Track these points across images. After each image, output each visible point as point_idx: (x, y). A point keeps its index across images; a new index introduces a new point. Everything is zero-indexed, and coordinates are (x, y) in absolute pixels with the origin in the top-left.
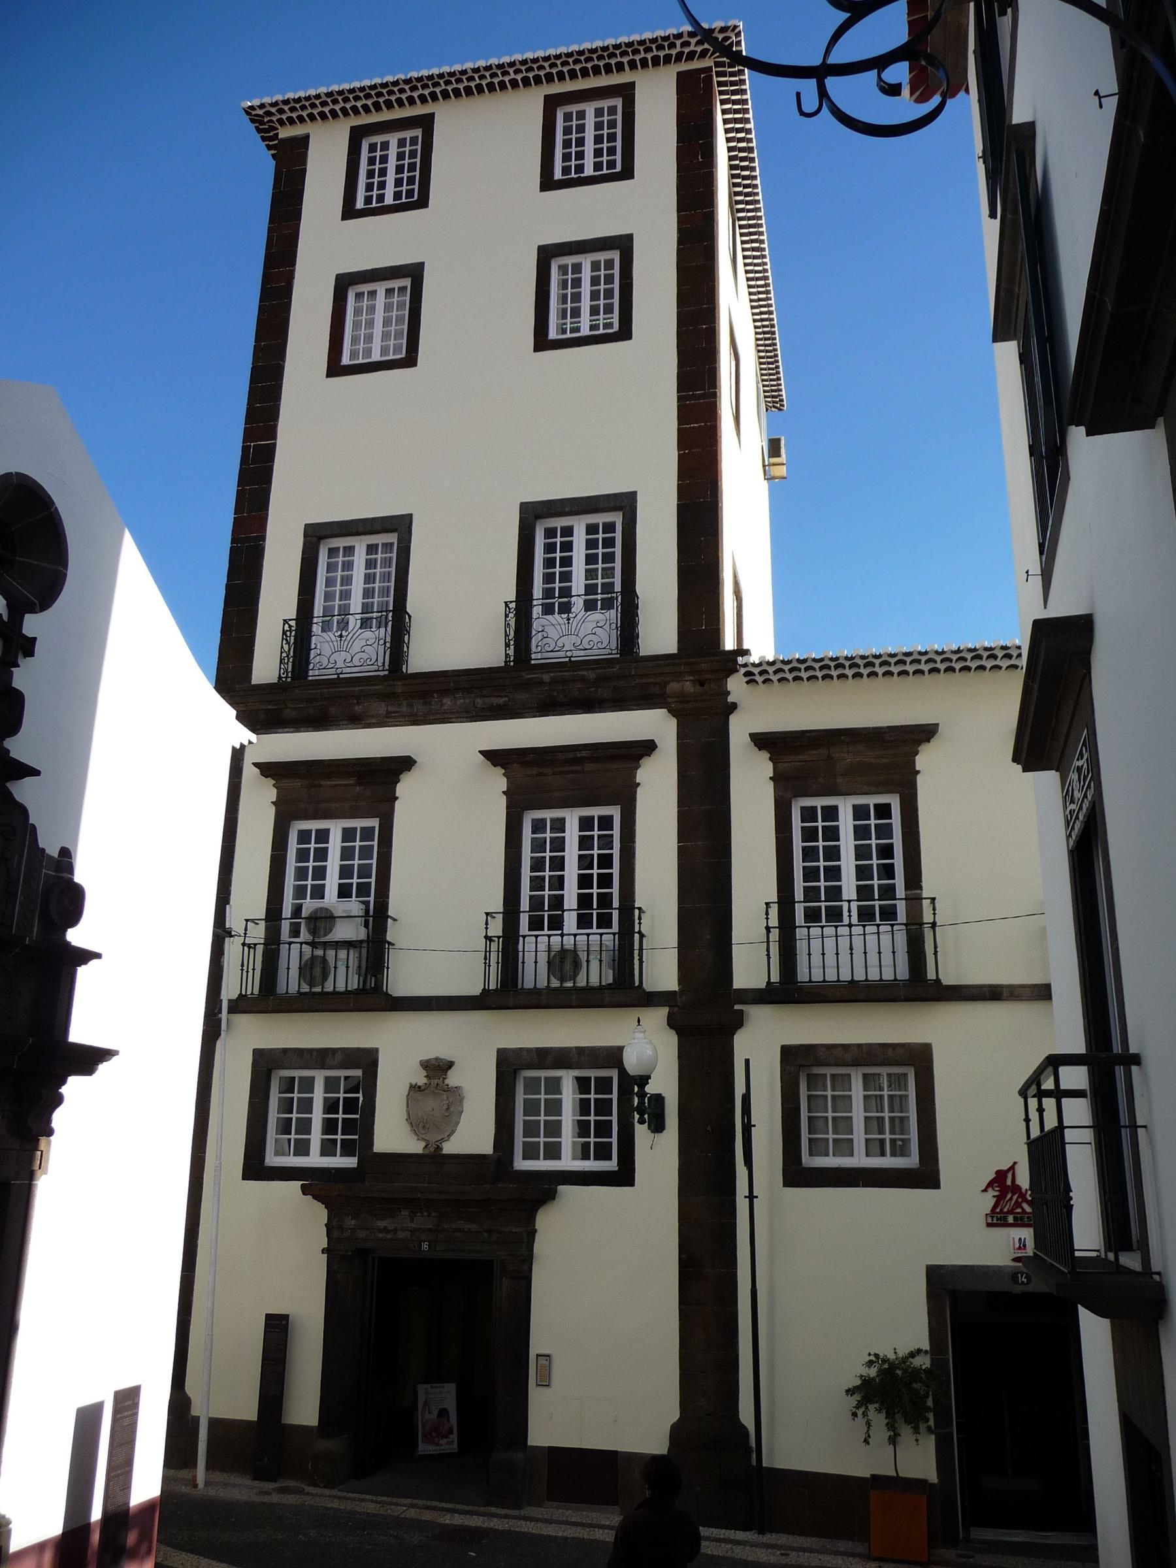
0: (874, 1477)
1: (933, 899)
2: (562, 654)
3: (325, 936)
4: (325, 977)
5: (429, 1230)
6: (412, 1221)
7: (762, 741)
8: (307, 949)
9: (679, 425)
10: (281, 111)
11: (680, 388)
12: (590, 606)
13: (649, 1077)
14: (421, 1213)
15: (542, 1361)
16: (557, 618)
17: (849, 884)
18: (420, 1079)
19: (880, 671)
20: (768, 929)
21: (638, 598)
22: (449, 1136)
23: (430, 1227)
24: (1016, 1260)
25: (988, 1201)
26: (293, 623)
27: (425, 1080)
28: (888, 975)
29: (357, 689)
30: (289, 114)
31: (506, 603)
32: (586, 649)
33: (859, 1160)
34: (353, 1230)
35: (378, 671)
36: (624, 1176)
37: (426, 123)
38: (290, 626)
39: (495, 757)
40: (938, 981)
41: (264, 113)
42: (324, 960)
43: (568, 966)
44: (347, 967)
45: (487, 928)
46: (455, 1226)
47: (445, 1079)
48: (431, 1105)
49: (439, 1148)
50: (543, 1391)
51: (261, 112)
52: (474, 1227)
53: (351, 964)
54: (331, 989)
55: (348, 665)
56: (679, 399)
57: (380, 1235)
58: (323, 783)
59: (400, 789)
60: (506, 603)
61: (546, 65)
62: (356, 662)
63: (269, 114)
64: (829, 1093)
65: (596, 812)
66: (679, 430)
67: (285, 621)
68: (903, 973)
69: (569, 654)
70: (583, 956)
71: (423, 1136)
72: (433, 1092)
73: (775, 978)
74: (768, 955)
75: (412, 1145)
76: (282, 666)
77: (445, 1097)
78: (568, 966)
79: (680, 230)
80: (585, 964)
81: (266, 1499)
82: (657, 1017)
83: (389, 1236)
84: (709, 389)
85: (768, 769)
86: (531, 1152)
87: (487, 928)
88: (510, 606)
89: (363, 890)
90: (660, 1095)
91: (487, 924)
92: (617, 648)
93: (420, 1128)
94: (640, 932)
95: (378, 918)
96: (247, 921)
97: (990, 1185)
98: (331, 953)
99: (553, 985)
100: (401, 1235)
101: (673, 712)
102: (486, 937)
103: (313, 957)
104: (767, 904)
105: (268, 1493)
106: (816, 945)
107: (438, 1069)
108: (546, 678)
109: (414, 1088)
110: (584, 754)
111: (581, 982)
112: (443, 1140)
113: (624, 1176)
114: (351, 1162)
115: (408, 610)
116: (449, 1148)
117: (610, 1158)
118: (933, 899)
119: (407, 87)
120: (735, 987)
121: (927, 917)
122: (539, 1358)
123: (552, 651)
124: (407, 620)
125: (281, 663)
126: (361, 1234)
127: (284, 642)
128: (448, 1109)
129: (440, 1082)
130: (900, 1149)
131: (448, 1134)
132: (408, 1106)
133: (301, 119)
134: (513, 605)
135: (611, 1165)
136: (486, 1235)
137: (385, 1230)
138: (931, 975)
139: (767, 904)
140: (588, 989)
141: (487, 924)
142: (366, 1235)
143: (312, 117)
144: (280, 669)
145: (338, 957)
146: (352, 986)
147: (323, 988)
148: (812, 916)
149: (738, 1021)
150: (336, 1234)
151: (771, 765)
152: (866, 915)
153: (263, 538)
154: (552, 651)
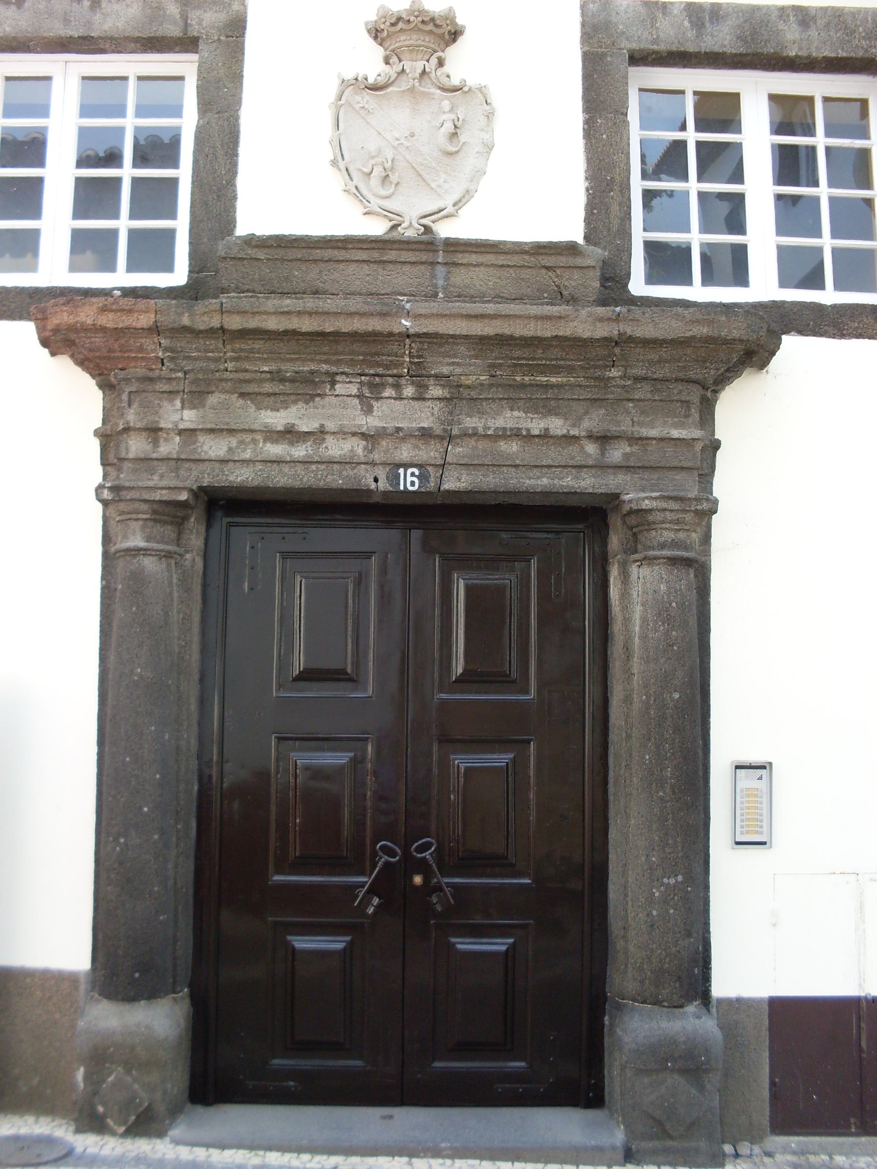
5: (425, 434)
6: (368, 410)
14: (397, 387)
15: (746, 779)
23: (425, 425)
27: (382, 67)
34: (188, 434)
46: (500, 422)
52: (557, 425)
57: (275, 450)
72: (412, 90)
77: (446, 105)
83: (300, 451)
93: (375, 181)
100: (335, 448)
122: (741, 773)
128: (454, 135)
131: (455, 197)
136: (591, 448)
137: (290, 434)
142: (230, 449)
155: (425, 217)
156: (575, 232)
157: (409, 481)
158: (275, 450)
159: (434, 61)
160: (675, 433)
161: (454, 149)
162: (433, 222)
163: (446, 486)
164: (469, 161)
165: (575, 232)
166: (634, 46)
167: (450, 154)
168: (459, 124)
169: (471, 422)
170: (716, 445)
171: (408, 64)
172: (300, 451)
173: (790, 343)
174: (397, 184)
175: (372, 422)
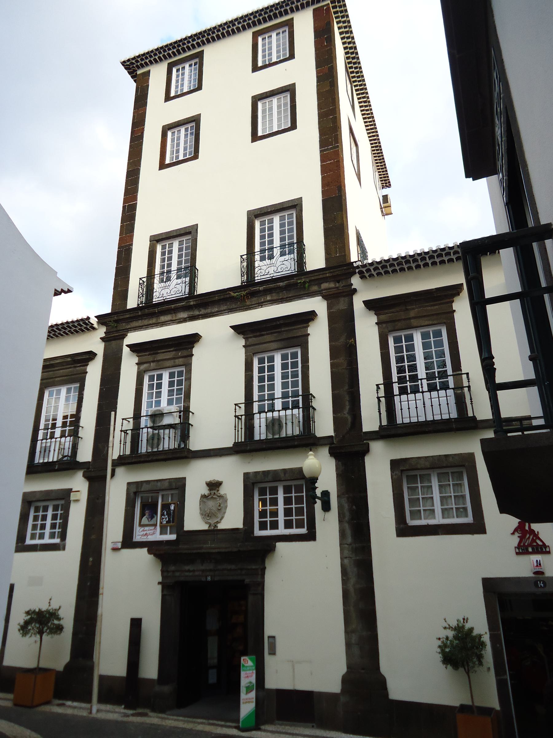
0: (462, 706)
1: (467, 374)
2: (268, 276)
3: (159, 423)
4: (158, 445)
5: (210, 570)
7: (370, 305)
8: (150, 430)
9: (321, 163)
10: (137, 61)
11: (321, 146)
12: (282, 254)
13: (317, 479)
15: (271, 640)
16: (267, 261)
17: (422, 372)
18: (205, 491)
19: (430, 262)
20: (378, 398)
21: (305, 246)
22: (221, 519)
24: (535, 573)
25: (515, 540)
26: (145, 280)
28: (446, 417)
29: (173, 306)
30: (141, 62)
31: (241, 256)
32: (279, 272)
33: (438, 520)
34: (173, 572)
35: (182, 295)
36: (311, 536)
37: (200, 55)
38: (143, 281)
39: (238, 329)
40: (474, 418)
41: (130, 63)
42: (158, 434)
43: (276, 427)
44: (169, 437)
45: (235, 412)
47: (219, 490)
48: (211, 504)
49: (216, 526)
50: (272, 657)
51: (128, 63)
52: (233, 567)
53: (171, 436)
54: (161, 449)
55: (169, 295)
56: (321, 151)
57: (187, 574)
58: (159, 351)
59: (195, 351)
60: (241, 256)
61: (252, 17)
62: (172, 293)
63: (133, 63)
64: (419, 485)
65: (289, 351)
66: (321, 166)
67: (140, 279)
68: (454, 415)
69: (271, 275)
70: (284, 422)
71: (208, 521)
72: (212, 497)
73: (385, 423)
74: (380, 414)
75: (204, 527)
76: (139, 299)
78: (276, 427)
79: (317, 77)
80: (284, 425)
81: (125, 719)
82: (325, 451)
84: (335, 144)
85: (375, 319)
86: (263, 526)
87: (235, 412)
88: (243, 257)
89: (178, 401)
90: (327, 491)
91: (235, 410)
92: (295, 269)
94: (312, 406)
95: (186, 412)
96: (123, 419)
97: (516, 530)
98: (162, 431)
99: (269, 438)
100: (197, 573)
101: (325, 297)
102: (235, 416)
103: (153, 434)
104: (377, 385)
105: (128, 716)
106: (405, 404)
107: (214, 486)
108: (261, 288)
109: (204, 497)
110: (282, 322)
111: (283, 435)
112: (218, 522)
113: (311, 536)
114: (173, 537)
115: (196, 267)
116: (221, 526)
117: (304, 527)
118: (467, 374)
119: (190, 40)
120: (364, 431)
121: (465, 384)
123: (263, 275)
124: (196, 271)
125: (139, 297)
126: (177, 574)
127: (140, 288)
128: (220, 506)
129: (216, 492)
130: (462, 512)
131: (220, 519)
132: (200, 505)
133: (147, 64)
134: (245, 257)
135: (303, 531)
137: (189, 571)
138: (470, 414)
139: (377, 385)
140: (287, 439)
141: (235, 410)
143: (151, 63)
144: (138, 301)
145: (165, 433)
146: (172, 446)
147: (158, 449)
148: (403, 391)
149: (366, 451)
150: (165, 574)
151: (376, 317)
152: (432, 388)
153: (132, 245)
154: (263, 275)
155: (215, 523)
156: (240, 525)
157: (209, 579)
158: (187, 574)
159: (216, 490)
160: (254, 567)
161: (220, 508)
162: (217, 524)
163: (216, 579)
164: (223, 510)
165: (240, 525)
166: (252, 482)
167: (219, 510)
168: (220, 503)
169: (220, 567)
170: (265, 568)
171: (212, 491)
172: (191, 574)
173: (280, 545)
174: (210, 517)
175: (203, 568)
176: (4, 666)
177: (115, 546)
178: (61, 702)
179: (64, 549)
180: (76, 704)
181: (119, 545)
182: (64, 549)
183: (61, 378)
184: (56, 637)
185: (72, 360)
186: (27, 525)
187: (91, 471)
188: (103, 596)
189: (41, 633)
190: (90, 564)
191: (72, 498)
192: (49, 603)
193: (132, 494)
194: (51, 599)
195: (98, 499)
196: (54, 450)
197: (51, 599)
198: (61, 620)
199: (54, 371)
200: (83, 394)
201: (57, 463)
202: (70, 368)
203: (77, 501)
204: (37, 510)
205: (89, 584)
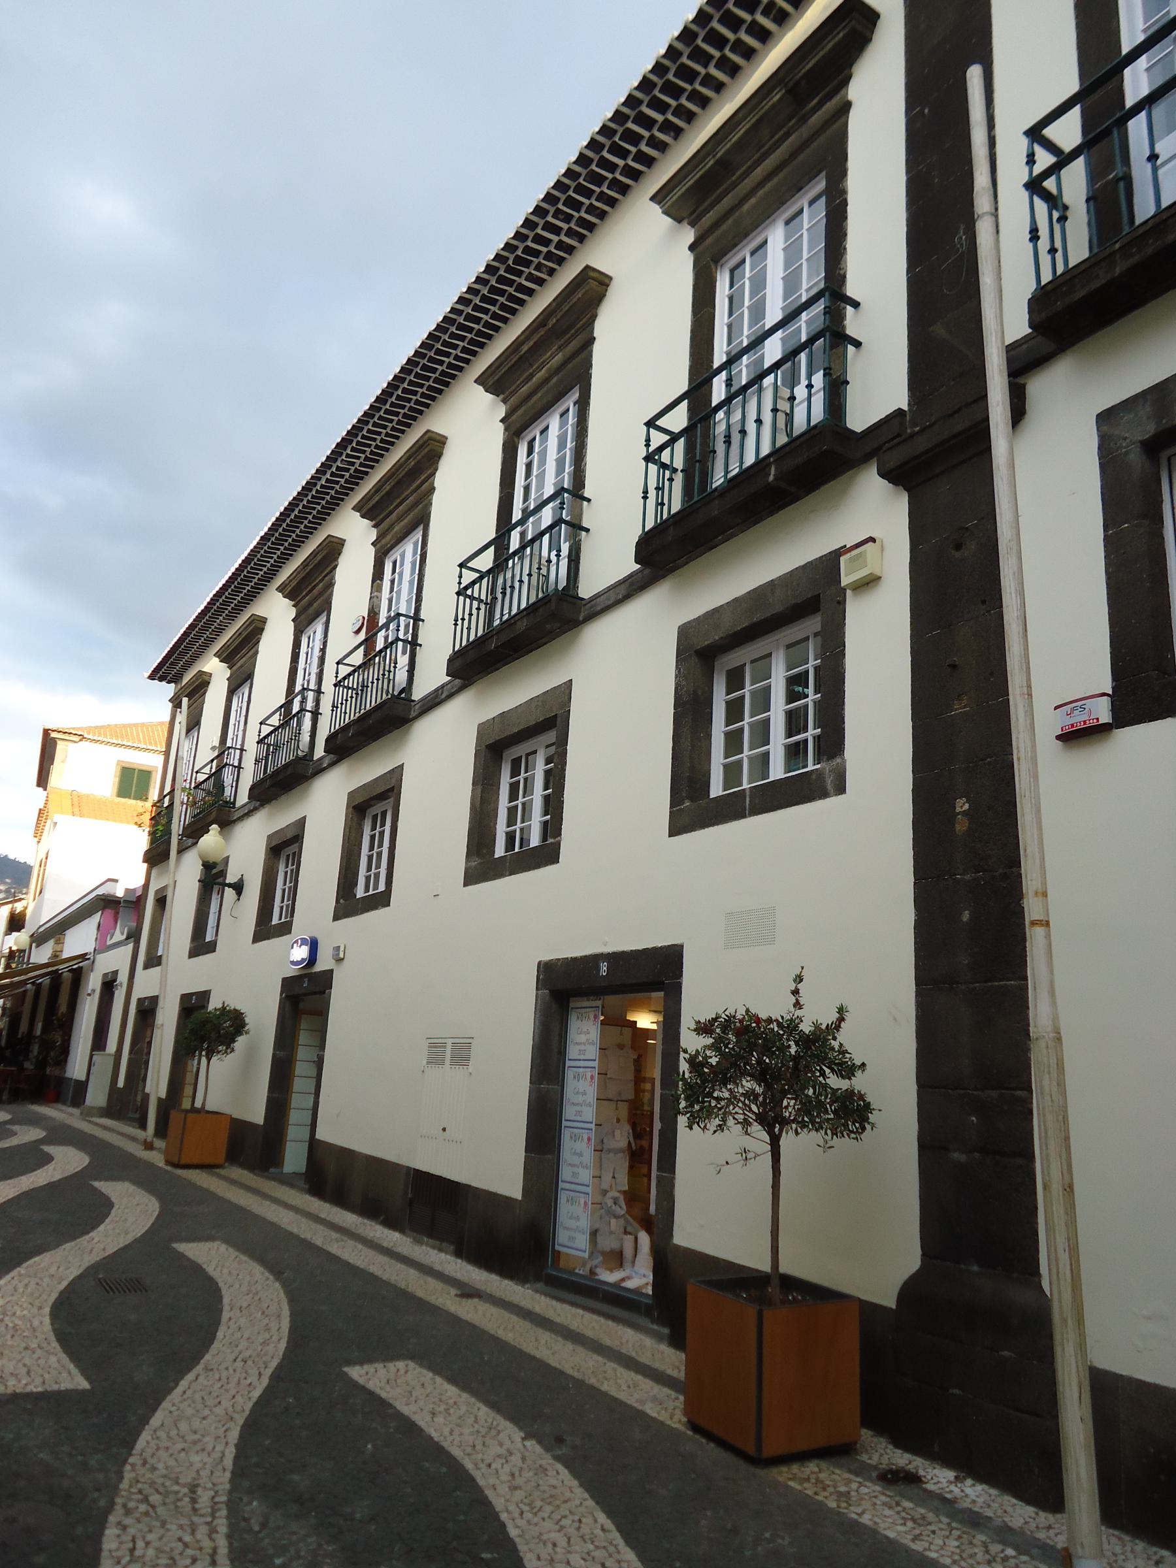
176: (678, 1247)
177: (1079, 719)
178: (901, 1459)
179: (841, 789)
180: (974, 1493)
181: (1102, 712)
182: (841, 789)
183: (761, 193)
184: (842, 1143)
185: (789, 92)
186: (709, 736)
187: (912, 436)
188: (1048, 936)
189: (773, 1122)
190: (961, 826)
191: (846, 579)
192: (796, 992)
193: (1136, 458)
194: (799, 979)
195: (958, 547)
196: (759, 421)
197: (799, 979)
198: (858, 1073)
199: (734, 185)
200: (844, 192)
201: (772, 460)
202: (787, 135)
203: (870, 583)
204: (735, 680)
205: (966, 916)
